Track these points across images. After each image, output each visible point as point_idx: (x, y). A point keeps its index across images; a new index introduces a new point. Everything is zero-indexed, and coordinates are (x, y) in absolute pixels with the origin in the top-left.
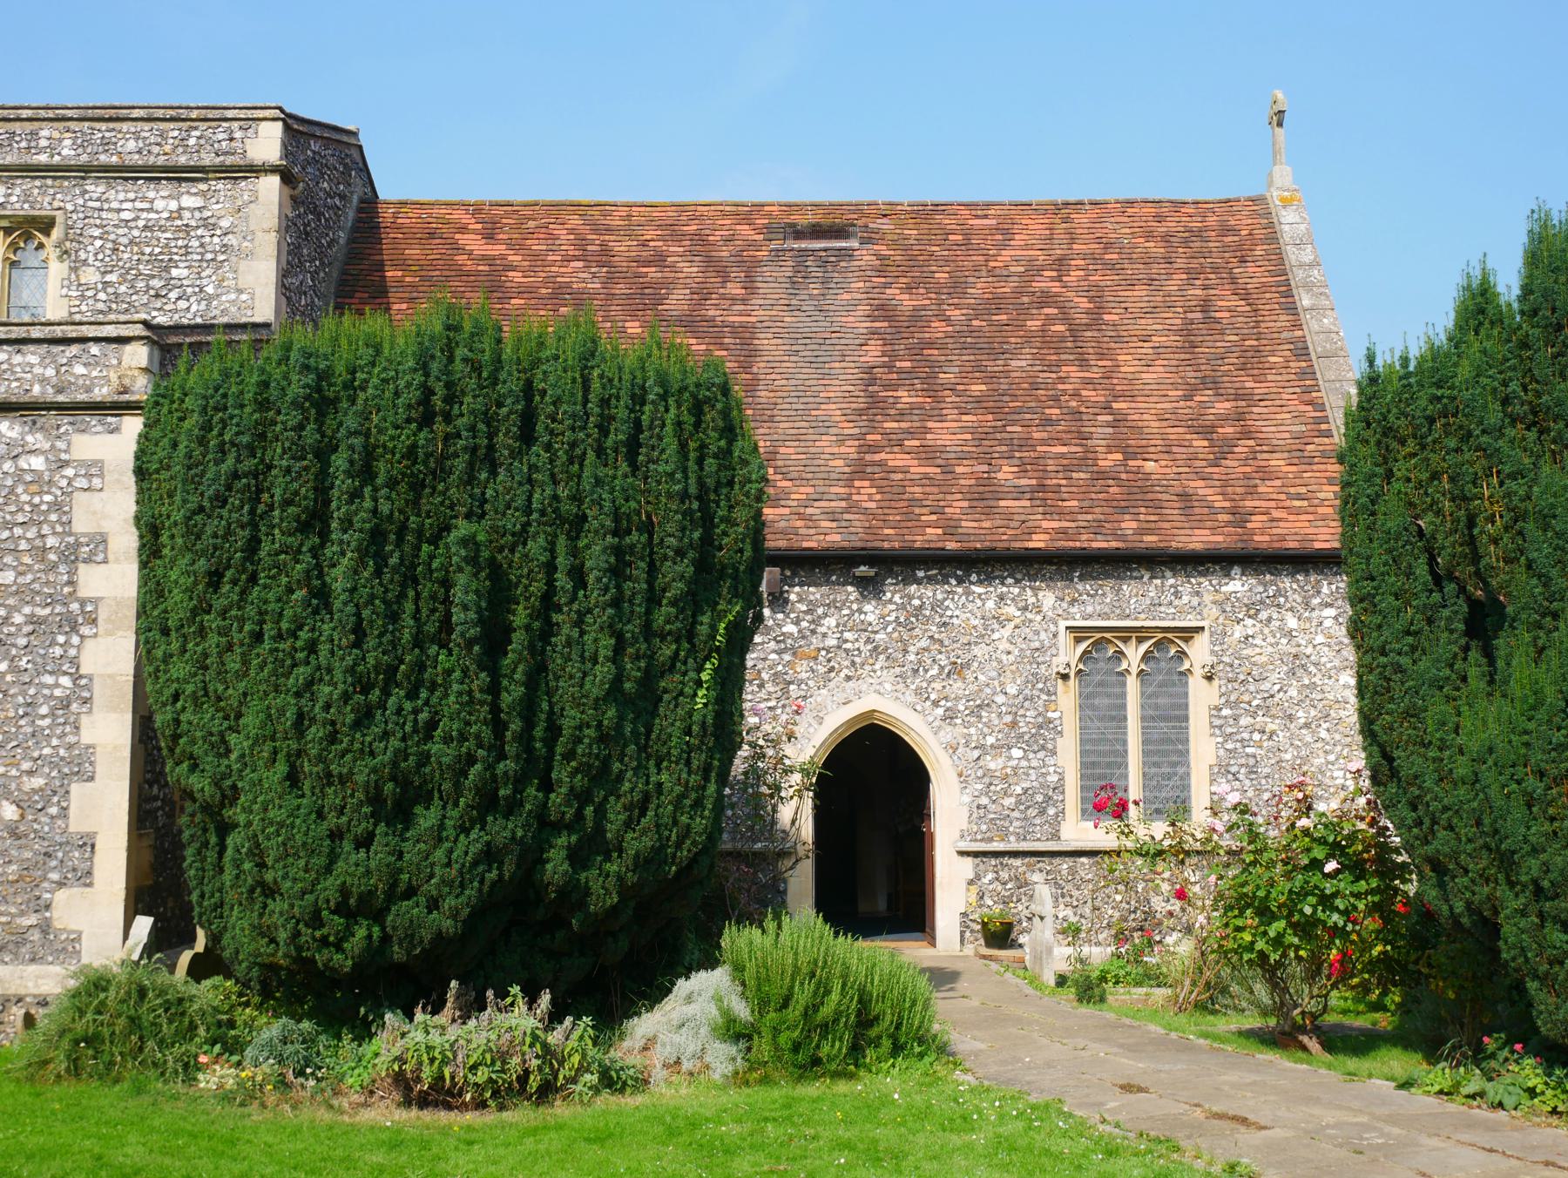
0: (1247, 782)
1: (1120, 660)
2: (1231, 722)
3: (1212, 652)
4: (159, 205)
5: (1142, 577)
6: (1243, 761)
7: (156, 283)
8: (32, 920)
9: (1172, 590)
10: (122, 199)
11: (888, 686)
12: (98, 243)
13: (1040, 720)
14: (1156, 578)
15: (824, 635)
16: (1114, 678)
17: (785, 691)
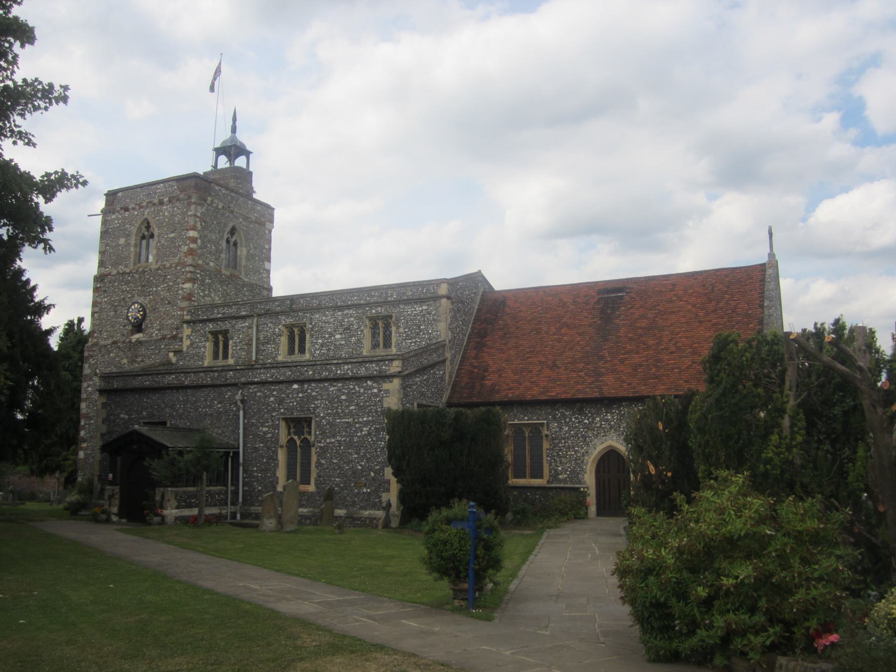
4: (417, 309)
7: (417, 331)
8: (377, 500)
10: (409, 310)
11: (615, 438)
12: (403, 321)
15: (596, 423)
17: (585, 440)
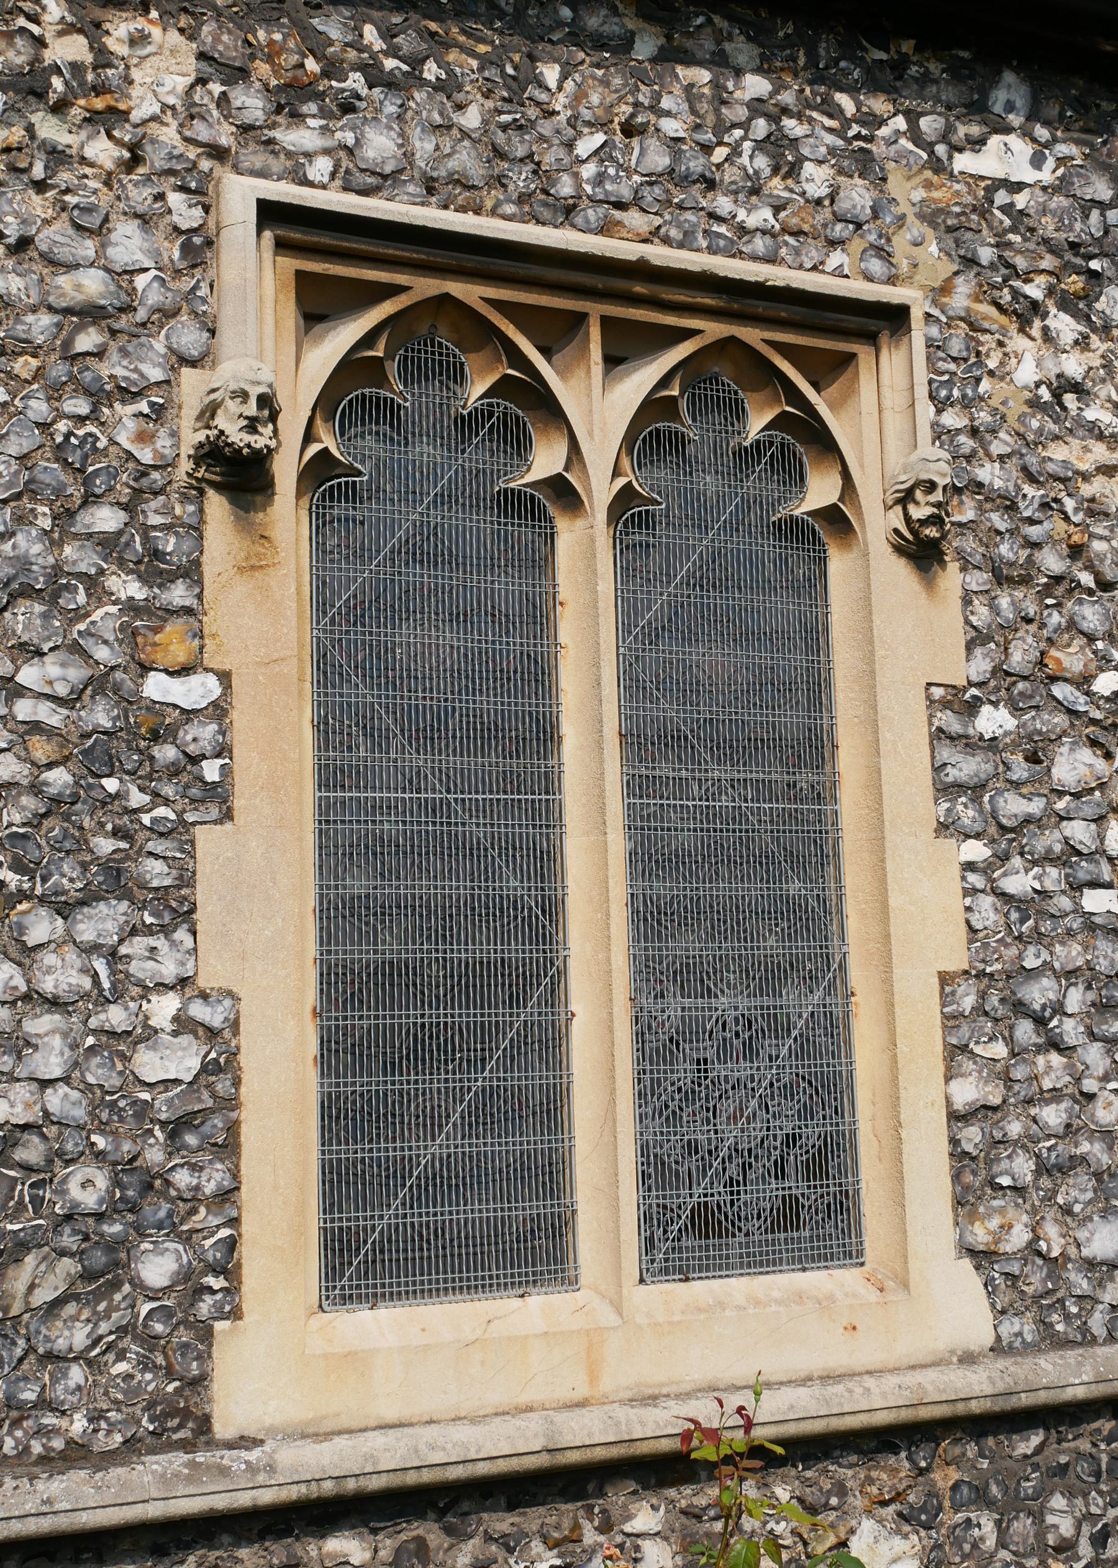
0: (1095, 1056)
1: (521, 447)
2: (1020, 770)
3: (940, 434)
5: (624, 45)
6: (1071, 954)
9: (761, 127)
13: (101, 715)
14: (690, 60)
16: (486, 522)
